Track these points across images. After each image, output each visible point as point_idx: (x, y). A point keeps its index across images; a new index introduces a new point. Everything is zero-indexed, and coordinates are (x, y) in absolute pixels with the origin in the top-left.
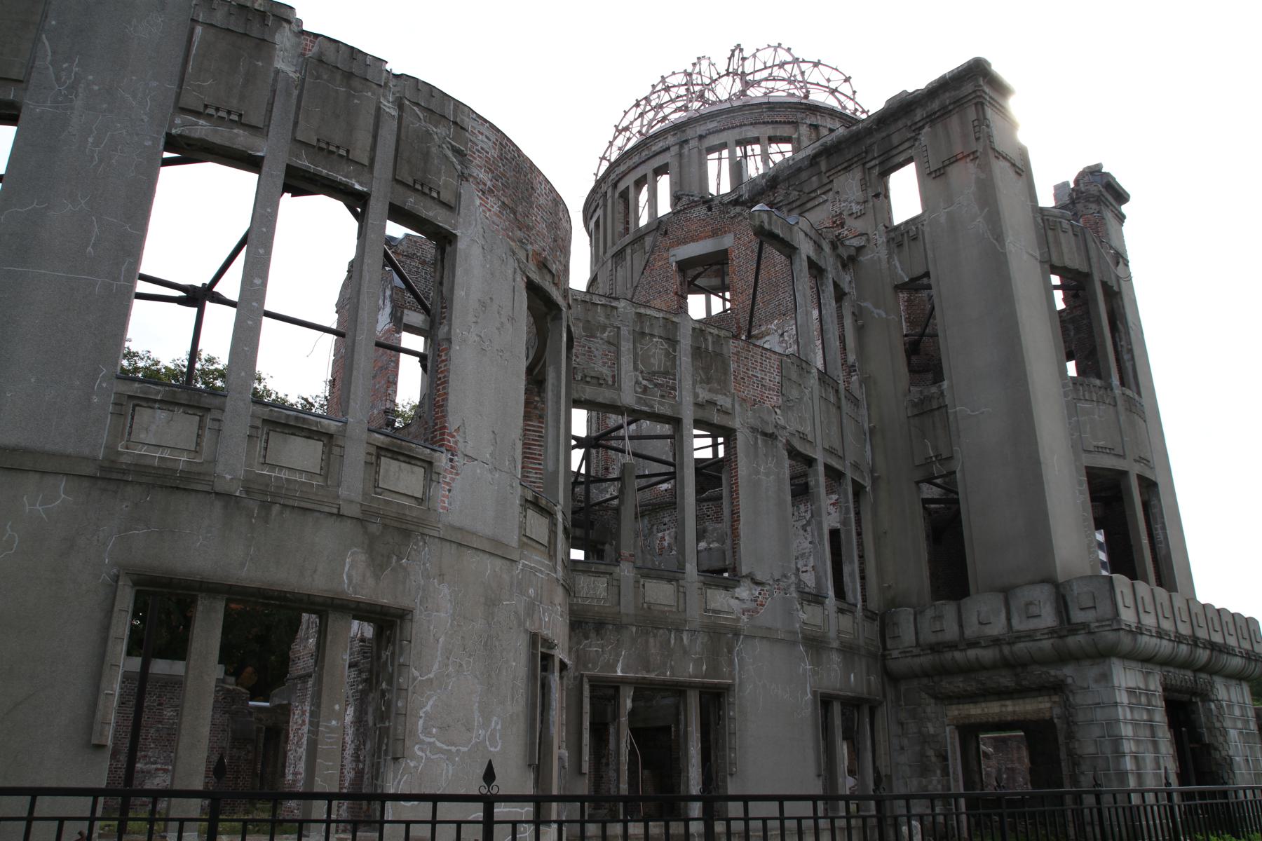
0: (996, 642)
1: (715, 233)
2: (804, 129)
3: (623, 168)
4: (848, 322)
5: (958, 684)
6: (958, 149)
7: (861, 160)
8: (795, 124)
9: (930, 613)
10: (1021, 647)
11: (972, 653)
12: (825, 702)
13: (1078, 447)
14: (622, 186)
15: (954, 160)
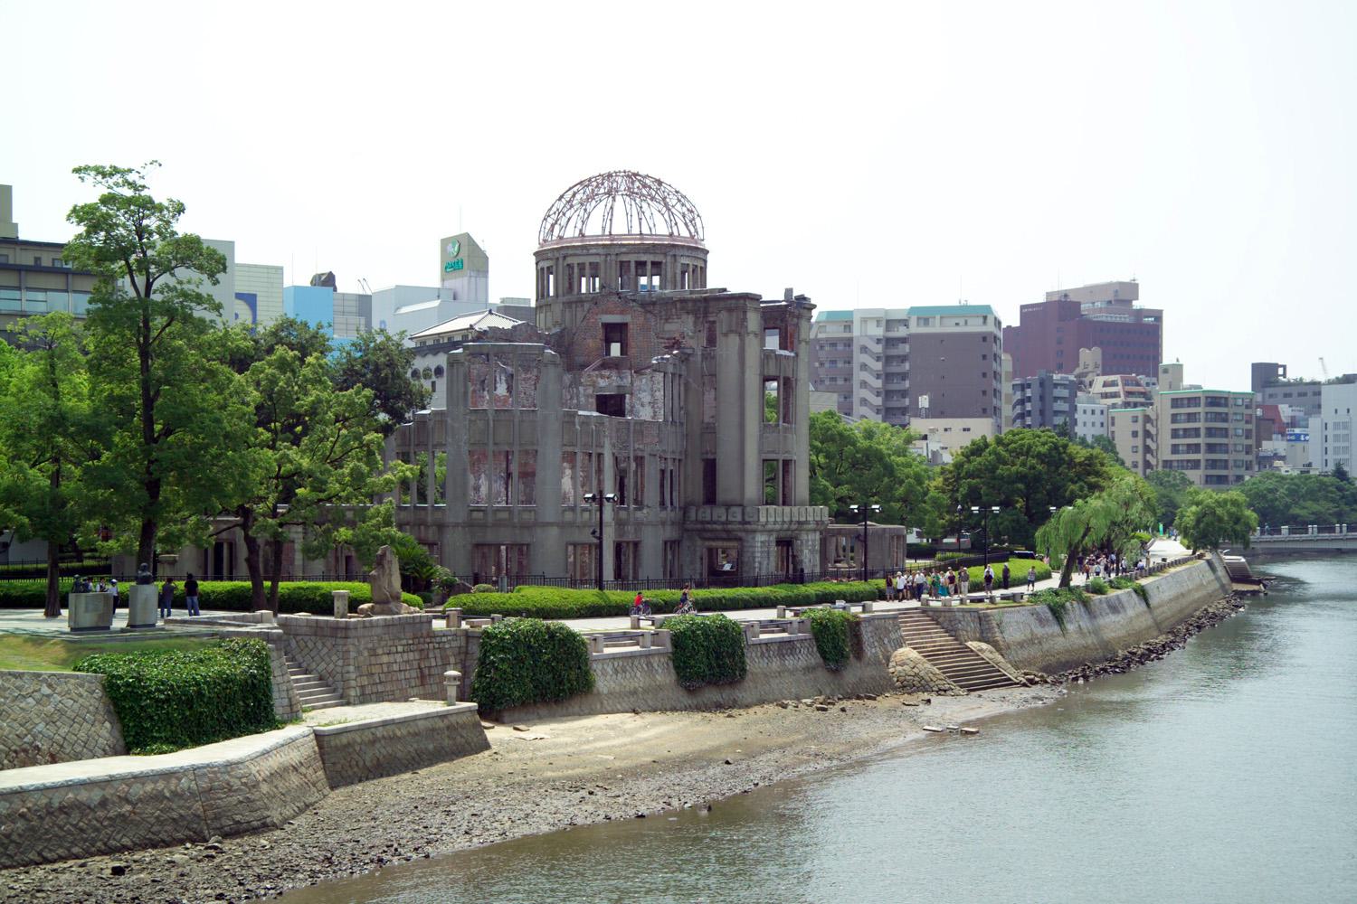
0: (723, 523)
1: (622, 313)
2: (669, 258)
3: (570, 252)
4: (682, 388)
5: (709, 535)
6: (734, 328)
7: (695, 313)
8: (665, 254)
9: (702, 510)
10: (730, 526)
11: (714, 526)
12: (666, 543)
13: (760, 451)
14: (569, 260)
15: (732, 331)
